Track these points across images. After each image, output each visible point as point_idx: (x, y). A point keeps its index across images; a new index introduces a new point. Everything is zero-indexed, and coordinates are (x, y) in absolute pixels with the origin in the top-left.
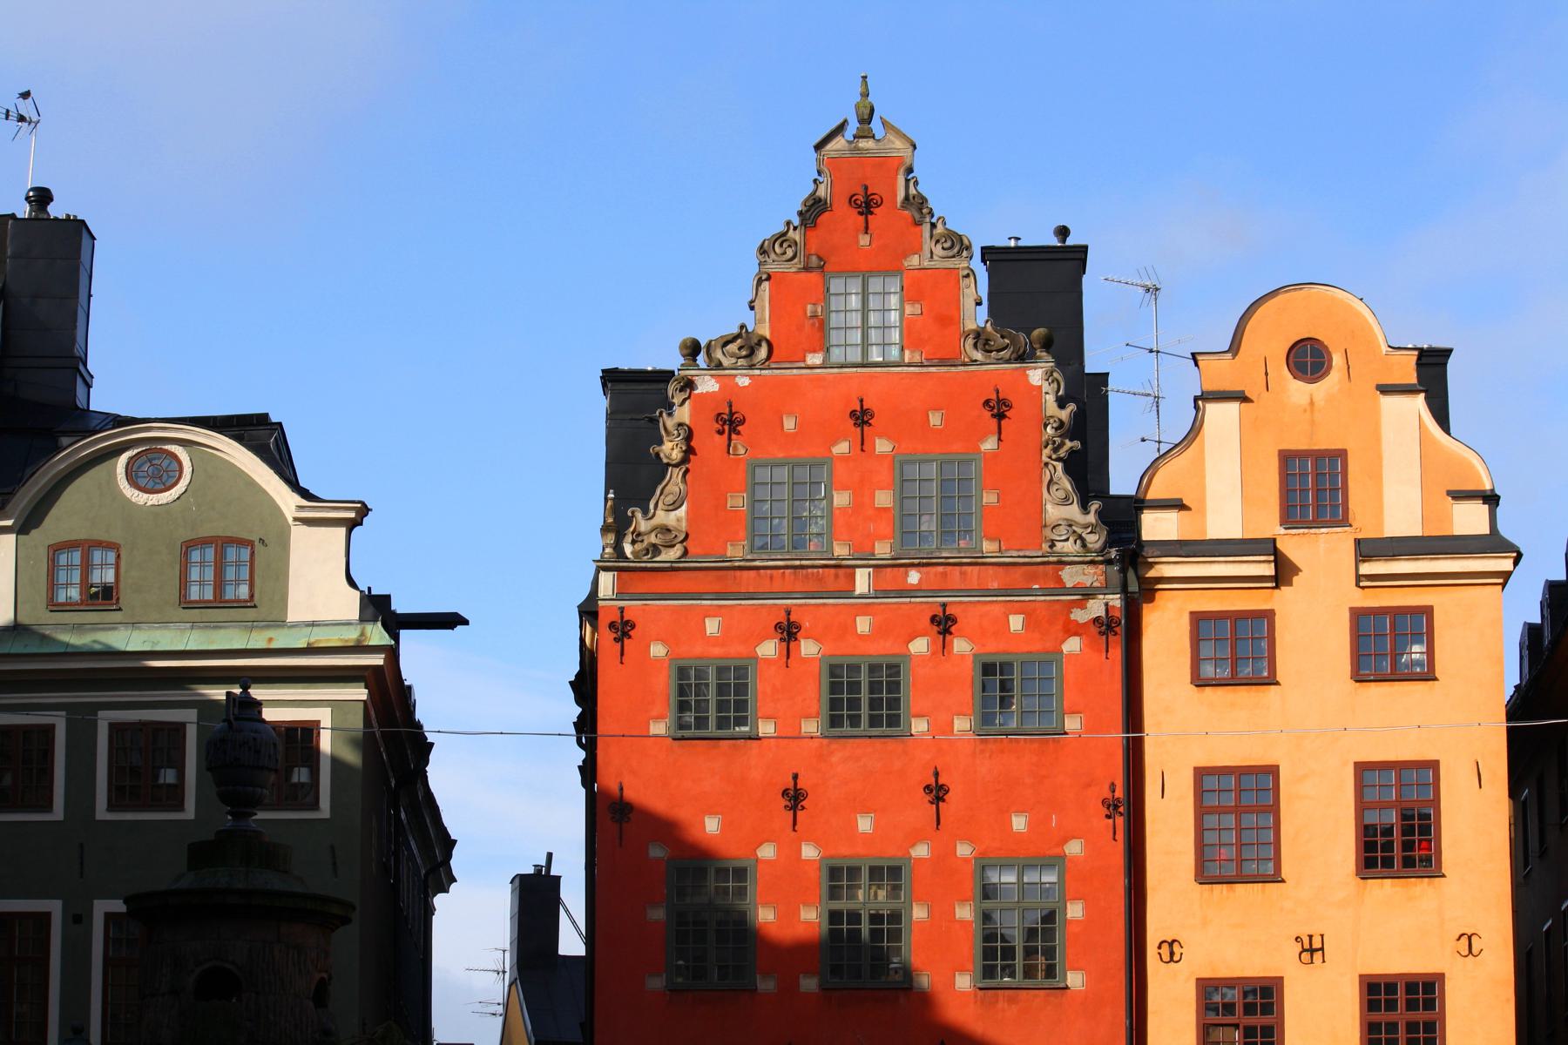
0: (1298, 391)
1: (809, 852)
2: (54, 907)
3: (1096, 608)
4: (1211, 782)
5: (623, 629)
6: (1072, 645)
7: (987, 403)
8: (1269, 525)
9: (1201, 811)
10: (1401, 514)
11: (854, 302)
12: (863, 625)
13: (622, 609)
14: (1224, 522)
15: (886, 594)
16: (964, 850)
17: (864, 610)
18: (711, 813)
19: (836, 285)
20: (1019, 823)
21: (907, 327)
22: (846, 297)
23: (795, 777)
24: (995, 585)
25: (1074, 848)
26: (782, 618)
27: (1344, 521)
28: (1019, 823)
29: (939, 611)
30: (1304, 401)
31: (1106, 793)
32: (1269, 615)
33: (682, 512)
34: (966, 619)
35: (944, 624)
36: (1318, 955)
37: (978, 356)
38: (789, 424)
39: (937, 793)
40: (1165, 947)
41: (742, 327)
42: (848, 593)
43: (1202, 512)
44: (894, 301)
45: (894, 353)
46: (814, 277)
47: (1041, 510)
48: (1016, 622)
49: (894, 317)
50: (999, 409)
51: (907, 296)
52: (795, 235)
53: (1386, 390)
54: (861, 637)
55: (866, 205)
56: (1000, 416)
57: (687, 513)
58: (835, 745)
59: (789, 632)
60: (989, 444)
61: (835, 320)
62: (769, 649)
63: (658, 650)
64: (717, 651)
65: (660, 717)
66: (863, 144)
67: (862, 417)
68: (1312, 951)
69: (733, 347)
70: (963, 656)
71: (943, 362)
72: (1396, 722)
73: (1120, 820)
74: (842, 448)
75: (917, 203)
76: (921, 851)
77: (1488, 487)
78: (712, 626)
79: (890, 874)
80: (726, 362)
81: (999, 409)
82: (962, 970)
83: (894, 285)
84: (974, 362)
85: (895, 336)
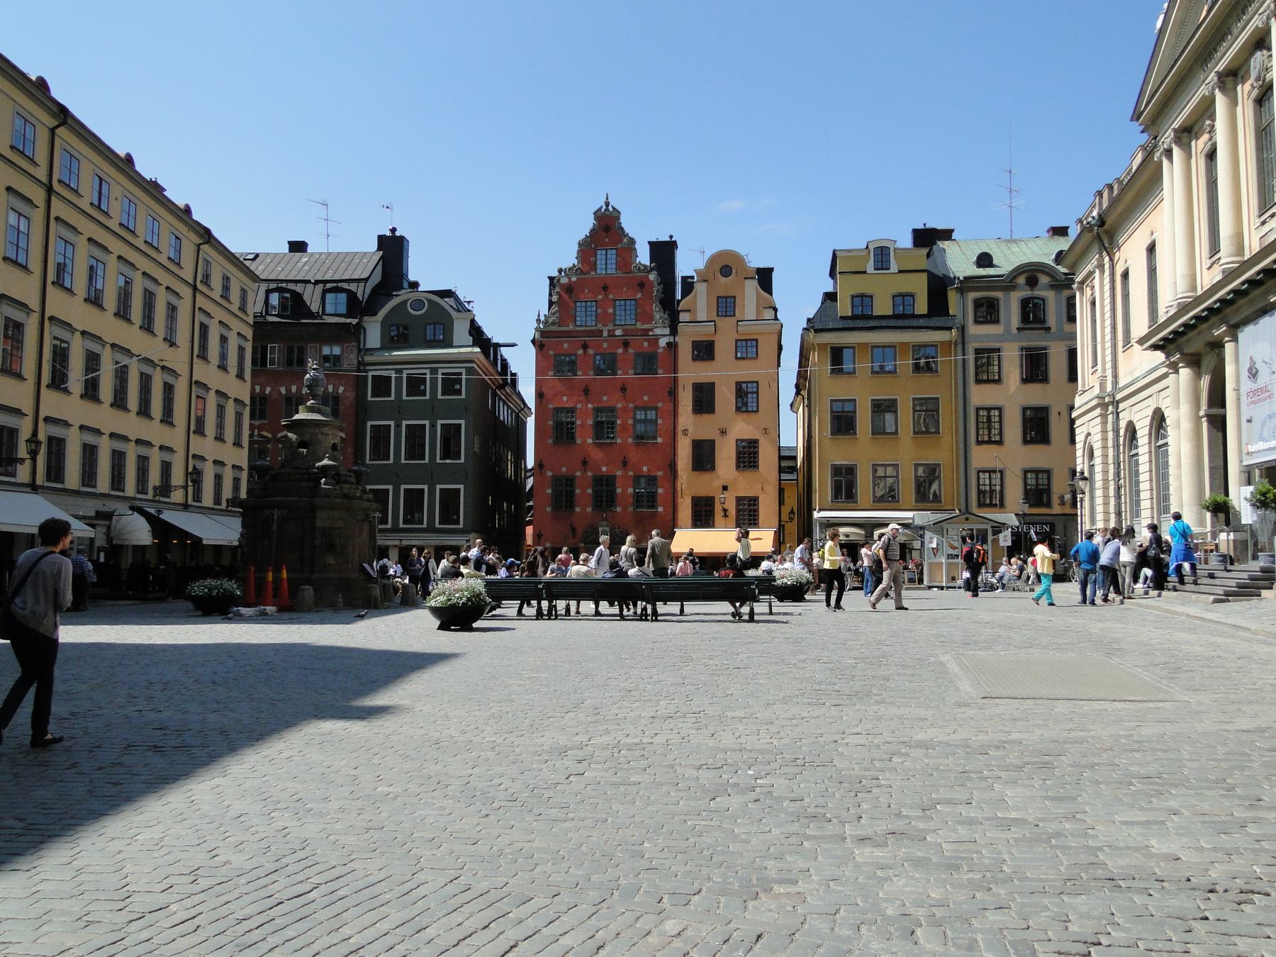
2: (392, 423)
8: (716, 318)
12: (605, 345)
14: (702, 316)
20: (646, 398)
25: (660, 405)
28: (646, 398)
35: (626, 344)
48: (646, 344)
59: (585, 347)
62: (580, 352)
63: (551, 352)
67: (605, 288)
72: (747, 371)
76: (619, 406)
78: (566, 346)
79: (612, 410)
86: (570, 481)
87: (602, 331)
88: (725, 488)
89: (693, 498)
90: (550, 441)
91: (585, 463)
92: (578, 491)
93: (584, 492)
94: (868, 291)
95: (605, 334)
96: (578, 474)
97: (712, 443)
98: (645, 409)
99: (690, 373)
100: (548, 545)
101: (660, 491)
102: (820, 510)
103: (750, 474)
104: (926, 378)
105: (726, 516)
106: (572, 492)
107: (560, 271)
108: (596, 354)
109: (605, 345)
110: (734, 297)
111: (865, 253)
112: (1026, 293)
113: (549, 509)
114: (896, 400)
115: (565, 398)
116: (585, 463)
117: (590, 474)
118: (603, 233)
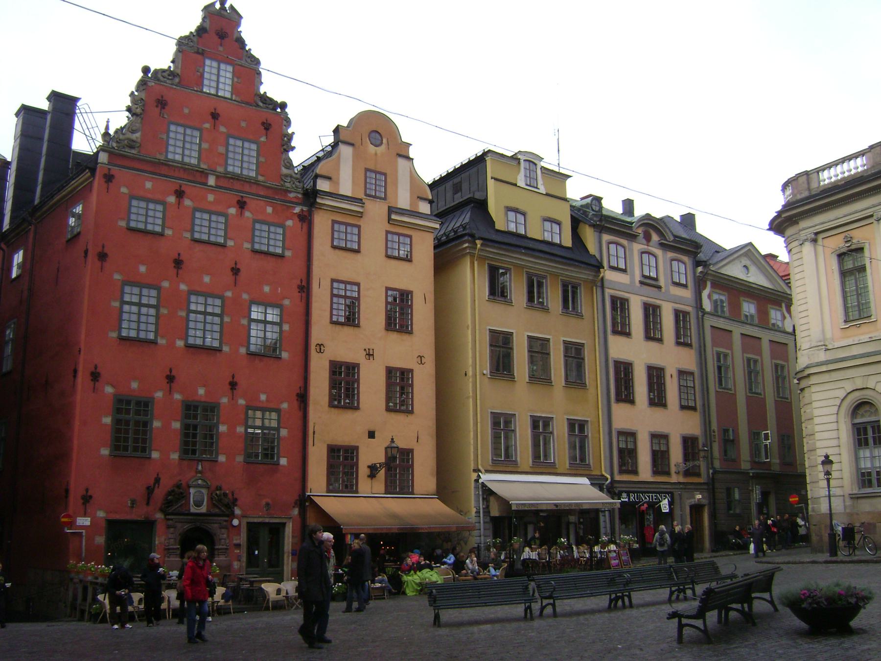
0: (372, 149)
1: (183, 287)
3: (297, 210)
4: (335, 285)
5: (109, 178)
6: (289, 223)
7: (263, 124)
8: (361, 195)
9: (333, 295)
10: (403, 200)
11: (215, 71)
13: (109, 169)
14: (346, 188)
15: (221, 187)
16: (245, 296)
17: (212, 191)
18: (143, 264)
19: (208, 62)
20: (267, 289)
21: (233, 86)
22: (210, 66)
23: (179, 254)
24: (262, 193)
25: (287, 302)
26: (177, 187)
27: (385, 199)
29: (240, 198)
30: (373, 152)
31: (299, 283)
32: (359, 227)
33: (138, 135)
34: (252, 203)
35: (242, 205)
36: (371, 358)
37: (261, 104)
38: (186, 111)
39: (236, 271)
40: (318, 348)
41: (170, 67)
42: (205, 184)
43: (337, 183)
44: (229, 75)
45: (228, 95)
46: (200, 57)
47: (280, 169)
48: (269, 210)
49: (229, 82)
50: (267, 126)
51: (234, 73)
52: (195, 39)
53: (400, 155)
54: (210, 203)
55: (222, 35)
56: (267, 129)
57: (142, 135)
58: (196, 245)
59: (180, 194)
60: (263, 139)
61: (206, 76)
62: (172, 199)
63: (124, 190)
64: (150, 196)
65: (123, 219)
66: (223, 12)
68: (369, 355)
69: (165, 74)
70: (248, 218)
71: (247, 103)
73: (304, 295)
74: (207, 126)
75: (241, 42)
76: (229, 294)
77: (430, 198)
80: (162, 79)
81: (267, 126)
82: (243, 346)
83: (230, 68)
84: (258, 106)
85: (229, 88)
86: (144, 405)
87: (207, 177)
88: (372, 435)
89: (328, 445)
90: (114, 335)
91: (170, 379)
92: (157, 424)
93: (167, 426)
94: (521, 207)
95: (212, 181)
96: (159, 395)
97: (352, 369)
98: (266, 304)
99: (327, 265)
100: (101, 514)
101: (284, 432)
102: (487, 471)
103: (400, 418)
104: (573, 321)
105: (372, 475)
106: (145, 424)
107: (146, 70)
108: (196, 209)
109: (211, 198)
110: (385, 174)
111: (514, 163)
112: (644, 247)
113: (105, 452)
114: (548, 340)
115: (143, 269)
116: (170, 379)
117: (177, 396)
118: (216, 39)
